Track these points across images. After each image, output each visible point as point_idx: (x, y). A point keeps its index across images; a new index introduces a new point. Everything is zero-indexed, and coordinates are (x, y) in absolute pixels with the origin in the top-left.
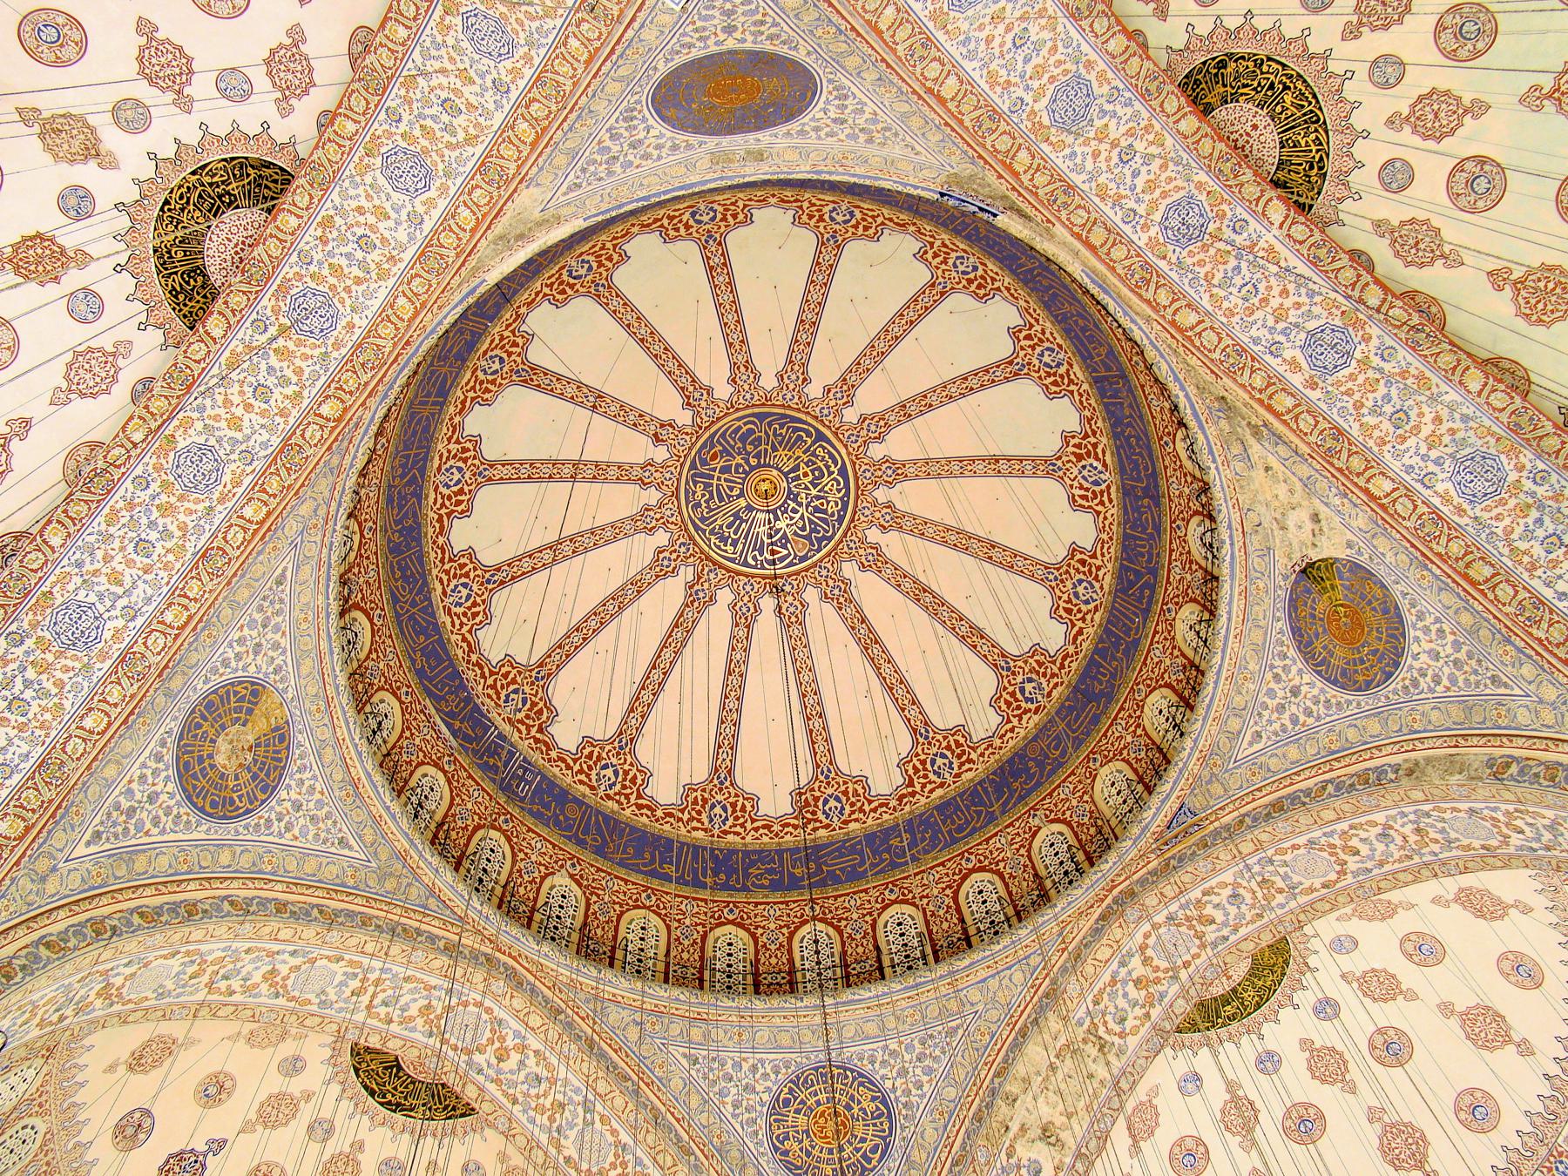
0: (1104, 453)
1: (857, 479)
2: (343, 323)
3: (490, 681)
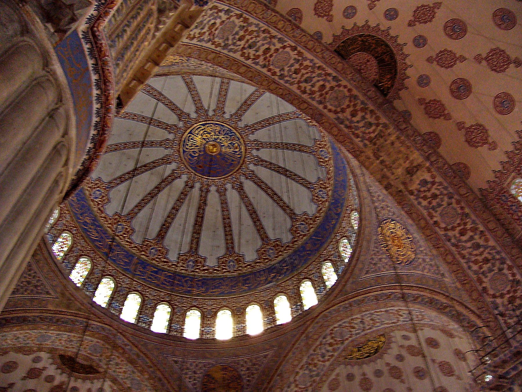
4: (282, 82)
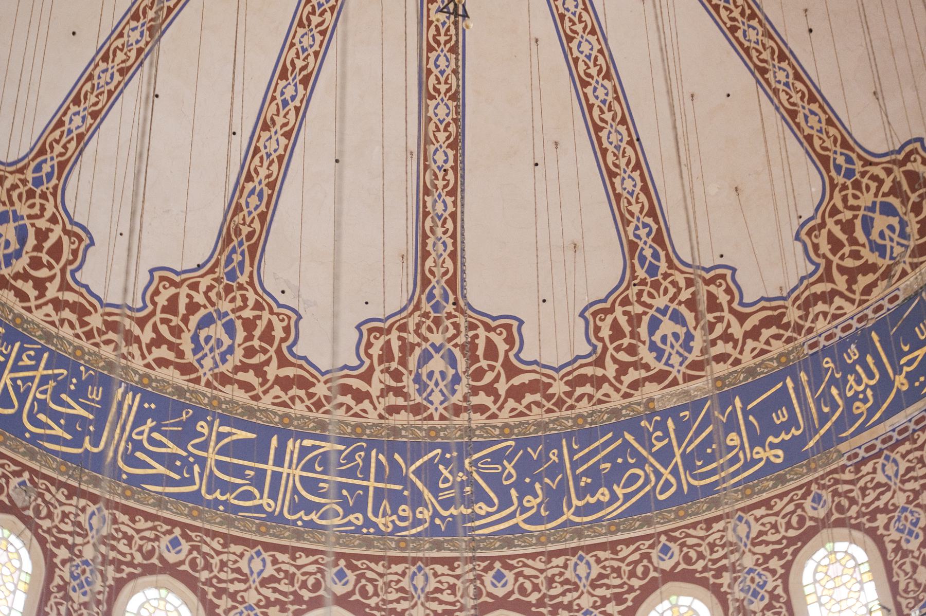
3: (841, 282)
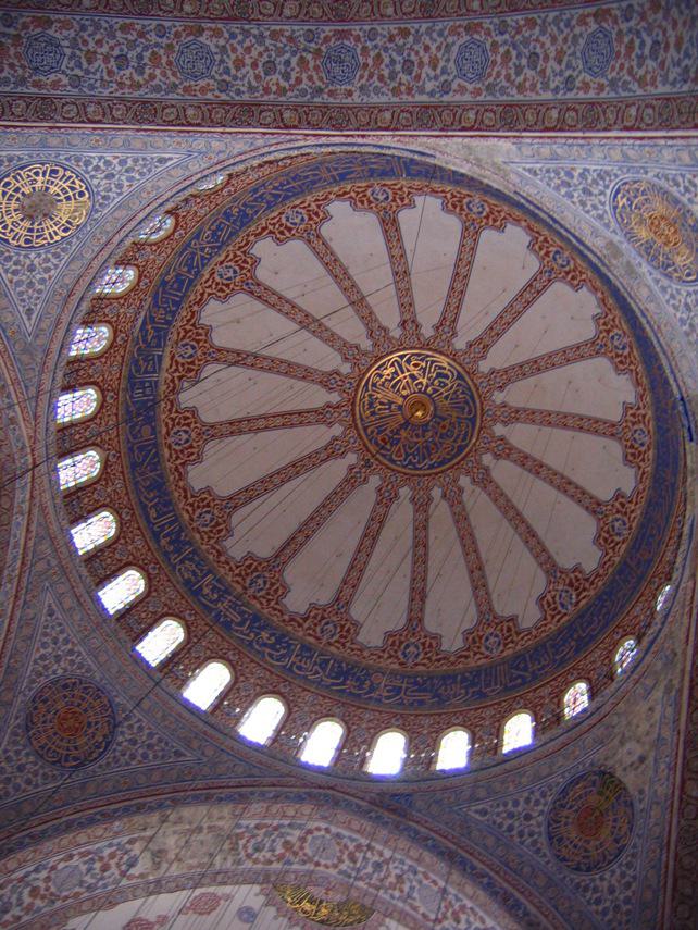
0: (584, 598)
1: (463, 459)
2: (349, 88)
3: (188, 328)
4: (408, 862)
